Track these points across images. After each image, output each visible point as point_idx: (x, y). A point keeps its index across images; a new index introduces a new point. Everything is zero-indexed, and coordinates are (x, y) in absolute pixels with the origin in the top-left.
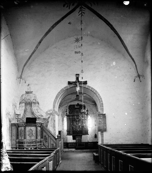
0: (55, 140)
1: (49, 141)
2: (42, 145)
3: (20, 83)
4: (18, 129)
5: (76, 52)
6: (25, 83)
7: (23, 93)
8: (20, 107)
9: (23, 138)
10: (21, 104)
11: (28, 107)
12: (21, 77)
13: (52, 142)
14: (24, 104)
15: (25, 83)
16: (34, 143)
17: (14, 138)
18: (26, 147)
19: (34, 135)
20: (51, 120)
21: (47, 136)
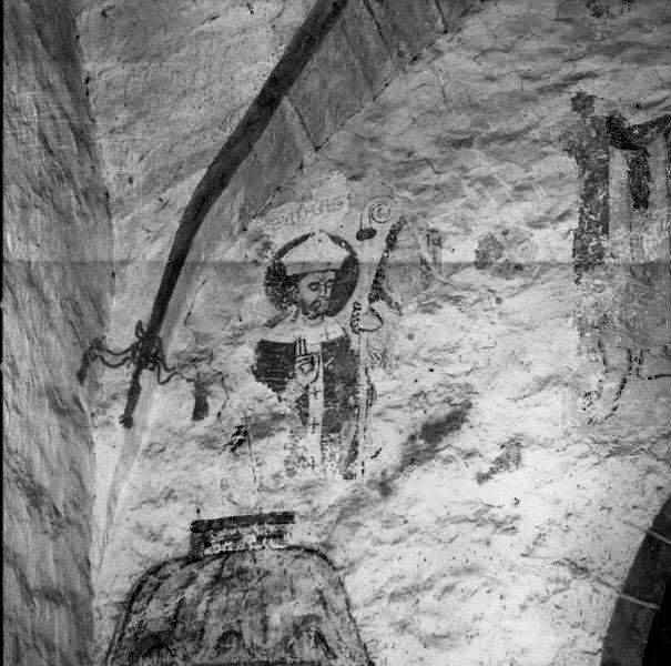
6: (200, 411)
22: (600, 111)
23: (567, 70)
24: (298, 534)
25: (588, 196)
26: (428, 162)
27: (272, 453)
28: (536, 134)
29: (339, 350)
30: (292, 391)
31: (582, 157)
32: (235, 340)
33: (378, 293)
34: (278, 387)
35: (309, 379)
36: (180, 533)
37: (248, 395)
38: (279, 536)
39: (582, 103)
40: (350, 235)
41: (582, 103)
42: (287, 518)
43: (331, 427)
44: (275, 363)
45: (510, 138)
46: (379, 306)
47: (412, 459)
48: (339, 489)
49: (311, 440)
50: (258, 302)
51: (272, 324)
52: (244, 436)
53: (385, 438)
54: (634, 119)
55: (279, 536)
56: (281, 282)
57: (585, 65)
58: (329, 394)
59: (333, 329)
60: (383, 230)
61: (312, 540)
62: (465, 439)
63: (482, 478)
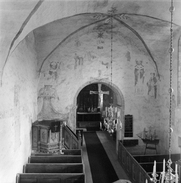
0: (77, 140)
1: (71, 141)
2: (63, 145)
3: (39, 77)
4: (40, 131)
5: (98, 48)
6: (45, 76)
7: (42, 87)
8: (38, 101)
9: (46, 142)
10: (39, 99)
11: (47, 102)
12: (40, 71)
13: (74, 142)
14: (42, 99)
15: (45, 76)
16: (57, 145)
17: (36, 139)
18: (49, 151)
19: (57, 137)
20: (71, 116)
21: (69, 136)
22: (77, 55)
23: (75, 51)
24: (53, 87)
25: (75, 63)
26: (63, 57)
27: (51, 80)
28: (72, 56)
29: (56, 72)
30: (52, 75)
31: (75, 60)
32: (47, 70)
33: (59, 68)
34: (51, 75)
35: (53, 75)
36: (43, 86)
37: (48, 75)
38: (51, 87)
39: (76, 54)
40: (57, 62)
41: (76, 54)
42: (52, 86)
43: (55, 79)
44: (51, 73)
45: (70, 56)
46: (59, 69)
47: (61, 83)
48: (56, 84)
49: (54, 80)
50: (49, 67)
51: (50, 69)
52: (48, 79)
53: (60, 80)
54: (80, 57)
55: (51, 87)
56: (51, 66)
57: (76, 51)
58: (55, 76)
59: (55, 71)
60: (59, 63)
61: (54, 88)
62: (65, 81)
63: (67, 85)
